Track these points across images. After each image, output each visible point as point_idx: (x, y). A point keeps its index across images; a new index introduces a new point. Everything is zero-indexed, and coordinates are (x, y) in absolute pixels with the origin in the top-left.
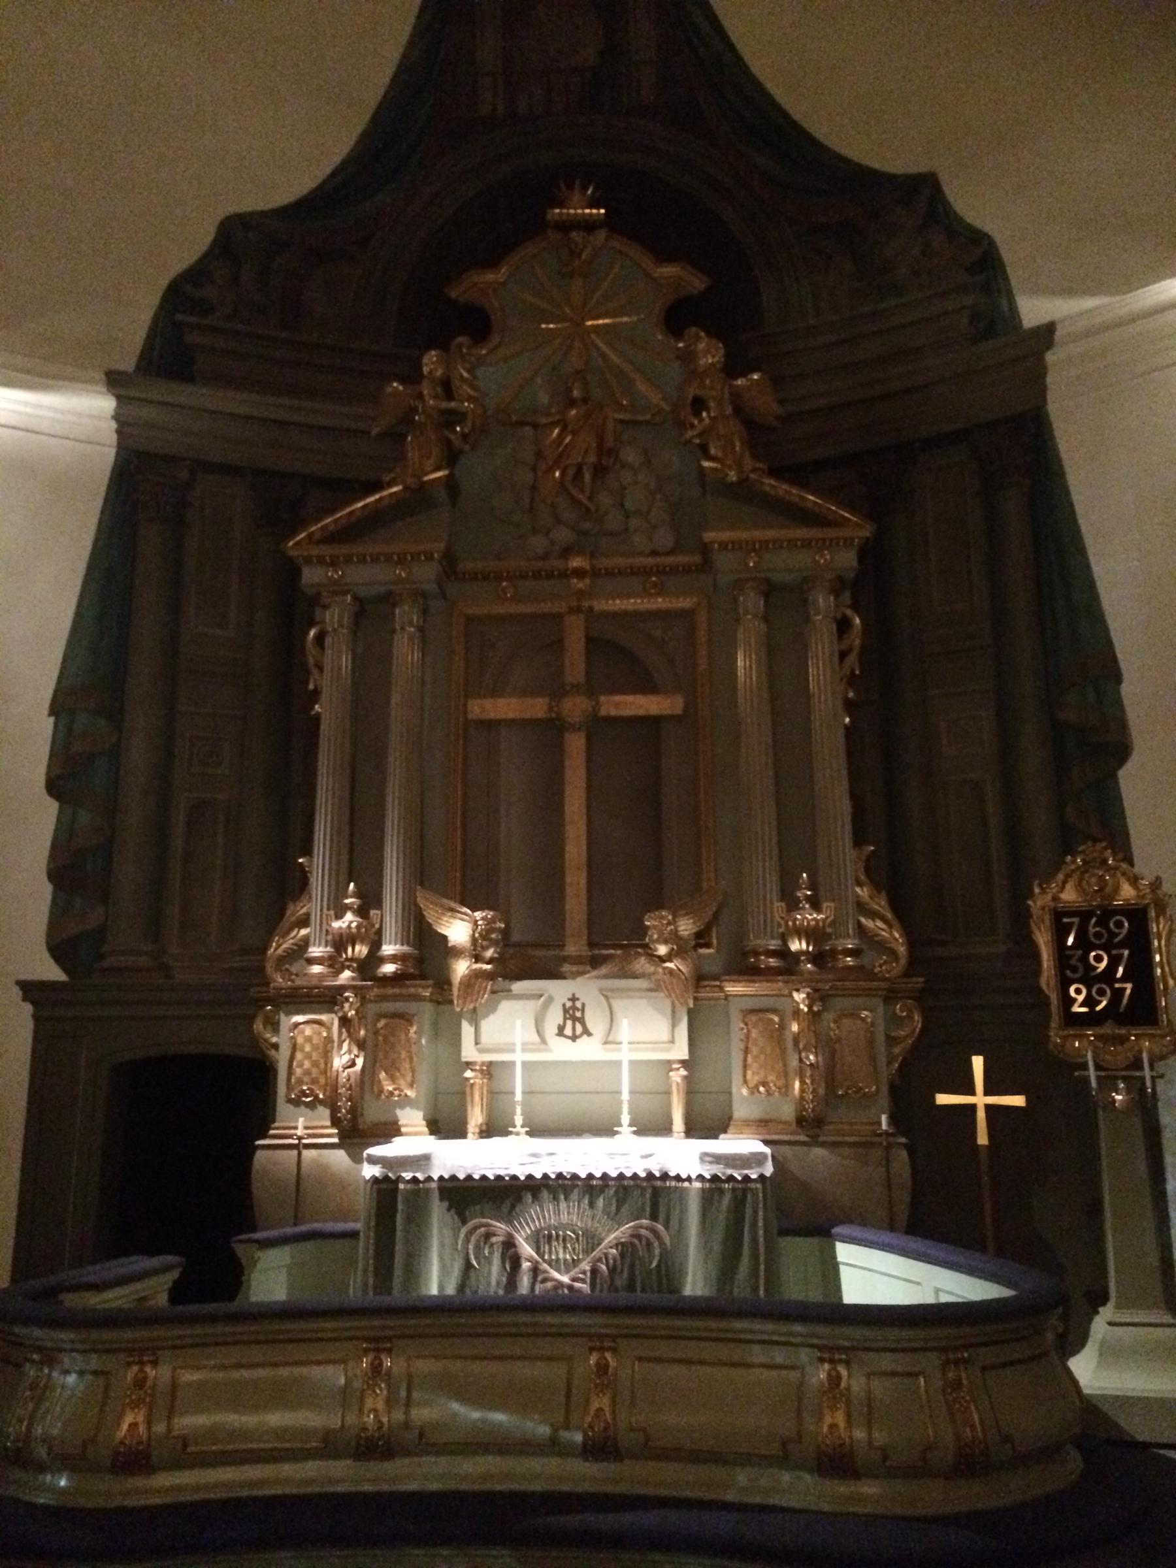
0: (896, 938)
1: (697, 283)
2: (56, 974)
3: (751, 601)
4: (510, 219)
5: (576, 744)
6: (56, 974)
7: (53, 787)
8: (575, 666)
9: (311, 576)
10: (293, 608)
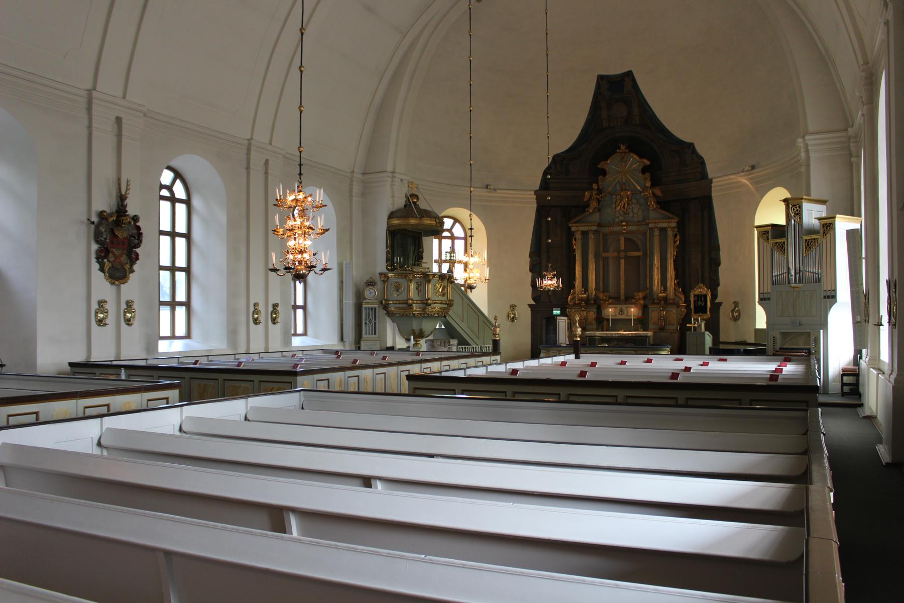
0: (682, 297)
1: (648, 163)
2: (533, 303)
3: (657, 233)
4: (608, 152)
5: (622, 261)
6: (533, 303)
7: (531, 270)
8: (622, 247)
9: (573, 229)
10: (570, 235)
